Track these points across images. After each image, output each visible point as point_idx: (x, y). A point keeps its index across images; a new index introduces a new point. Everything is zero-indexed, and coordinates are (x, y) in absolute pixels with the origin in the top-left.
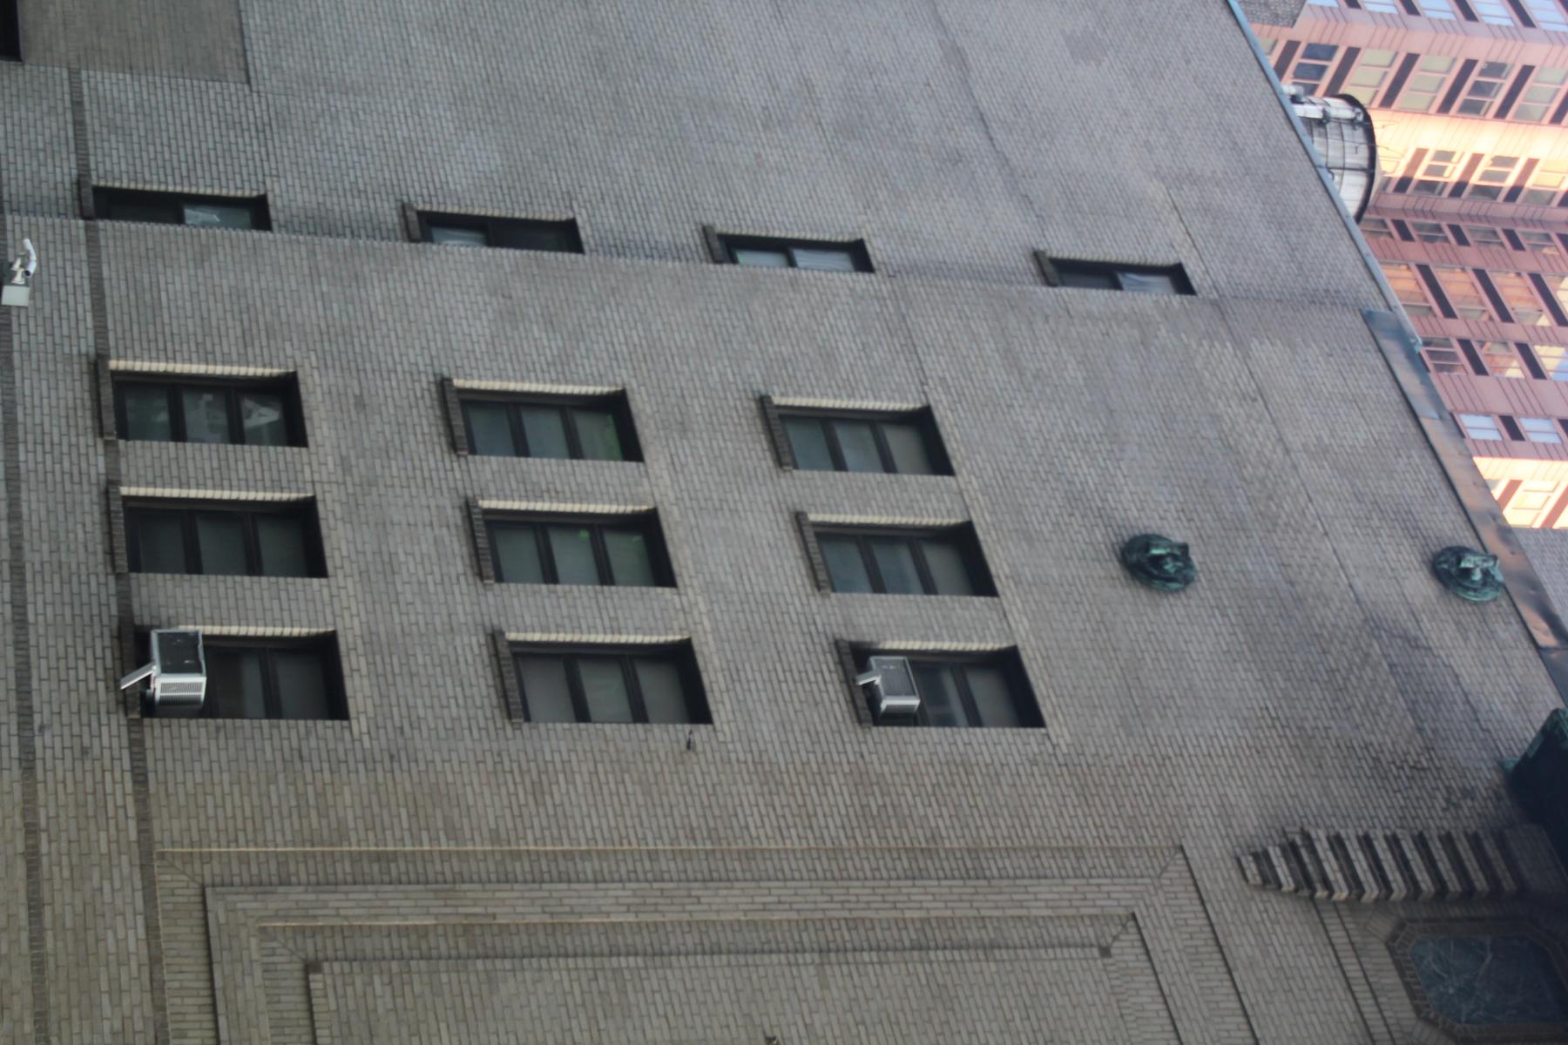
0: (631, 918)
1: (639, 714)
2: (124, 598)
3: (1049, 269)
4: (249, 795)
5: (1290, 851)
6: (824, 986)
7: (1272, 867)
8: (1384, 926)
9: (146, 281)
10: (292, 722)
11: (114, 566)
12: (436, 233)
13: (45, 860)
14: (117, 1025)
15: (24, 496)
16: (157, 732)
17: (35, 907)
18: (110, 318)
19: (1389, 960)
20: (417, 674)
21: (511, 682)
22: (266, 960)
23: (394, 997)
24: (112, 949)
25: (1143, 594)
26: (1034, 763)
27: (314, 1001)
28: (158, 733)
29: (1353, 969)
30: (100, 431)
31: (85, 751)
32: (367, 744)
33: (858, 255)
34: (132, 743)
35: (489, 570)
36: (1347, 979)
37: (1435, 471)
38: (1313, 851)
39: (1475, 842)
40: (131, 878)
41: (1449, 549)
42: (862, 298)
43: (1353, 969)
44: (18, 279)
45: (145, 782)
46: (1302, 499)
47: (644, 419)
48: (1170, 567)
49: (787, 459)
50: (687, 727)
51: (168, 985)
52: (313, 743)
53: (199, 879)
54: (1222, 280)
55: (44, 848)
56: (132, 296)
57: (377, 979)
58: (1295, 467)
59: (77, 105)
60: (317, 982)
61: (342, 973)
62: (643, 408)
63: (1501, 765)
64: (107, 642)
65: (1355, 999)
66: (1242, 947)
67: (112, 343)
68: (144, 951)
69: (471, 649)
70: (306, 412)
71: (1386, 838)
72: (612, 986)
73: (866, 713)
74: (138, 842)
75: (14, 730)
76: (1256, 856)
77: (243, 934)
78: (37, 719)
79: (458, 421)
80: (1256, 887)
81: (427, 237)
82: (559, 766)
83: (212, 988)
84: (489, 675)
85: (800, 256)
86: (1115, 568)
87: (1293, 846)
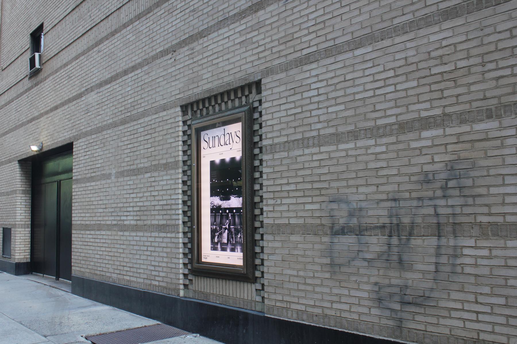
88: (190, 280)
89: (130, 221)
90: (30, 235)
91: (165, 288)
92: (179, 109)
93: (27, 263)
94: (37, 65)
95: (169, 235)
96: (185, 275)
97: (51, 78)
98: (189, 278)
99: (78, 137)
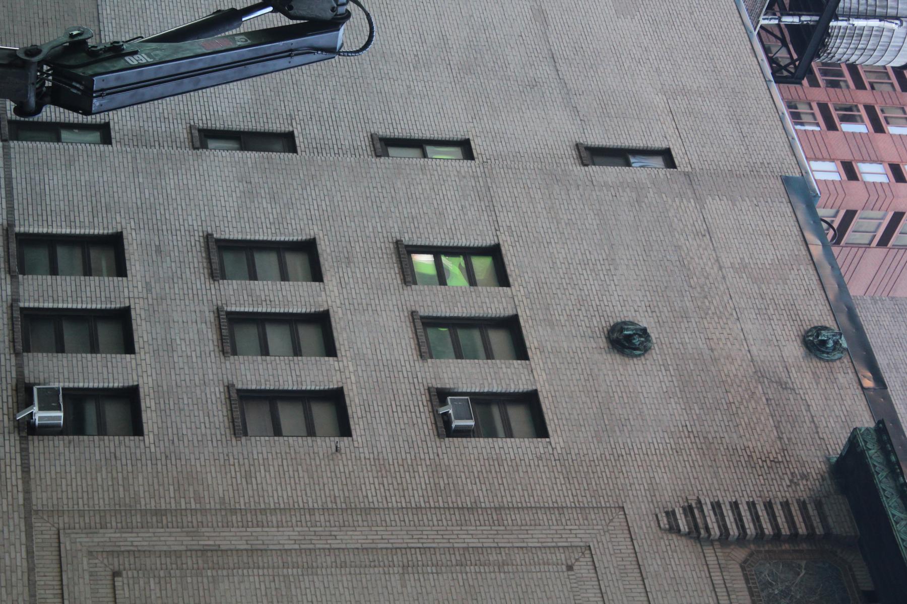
0: (297, 547)
1: (311, 432)
2: (20, 367)
3: (584, 154)
4: (86, 479)
5: (689, 510)
6: (404, 586)
7: (676, 520)
8: (740, 554)
9: (37, 178)
10: (111, 437)
11: (14, 350)
12: (212, 144)
16: (36, 444)
18: (16, 201)
19: (741, 574)
20: (184, 410)
21: (237, 414)
22: (91, 570)
23: (161, 590)
24: (8, 563)
25: (618, 358)
26: (540, 459)
27: (117, 592)
28: (37, 445)
29: (717, 579)
30: (9, 271)
32: (153, 450)
34: (22, 450)
35: (228, 348)
36: (713, 584)
37: (815, 278)
38: (702, 511)
39: (803, 505)
40: (19, 525)
41: (815, 328)
42: (464, 177)
43: (717, 579)
45: (29, 472)
47: (325, 256)
48: (637, 341)
49: (409, 279)
50: (337, 439)
51: (38, 583)
53: (56, 525)
54: (695, 158)
56: (29, 188)
57: (152, 580)
58: (724, 278)
60: (118, 584)
61: (133, 577)
64: (10, 393)
65: (717, 596)
66: (652, 565)
67: (17, 218)
68: (25, 564)
69: (215, 395)
70: (127, 256)
71: (748, 503)
72: (283, 584)
74: (24, 505)
76: (667, 513)
77: (80, 555)
79: (215, 259)
80: (665, 530)
81: (204, 146)
82: (261, 462)
83: (62, 585)
84: (225, 410)
85: (429, 149)
86: (603, 343)
87: (690, 507)
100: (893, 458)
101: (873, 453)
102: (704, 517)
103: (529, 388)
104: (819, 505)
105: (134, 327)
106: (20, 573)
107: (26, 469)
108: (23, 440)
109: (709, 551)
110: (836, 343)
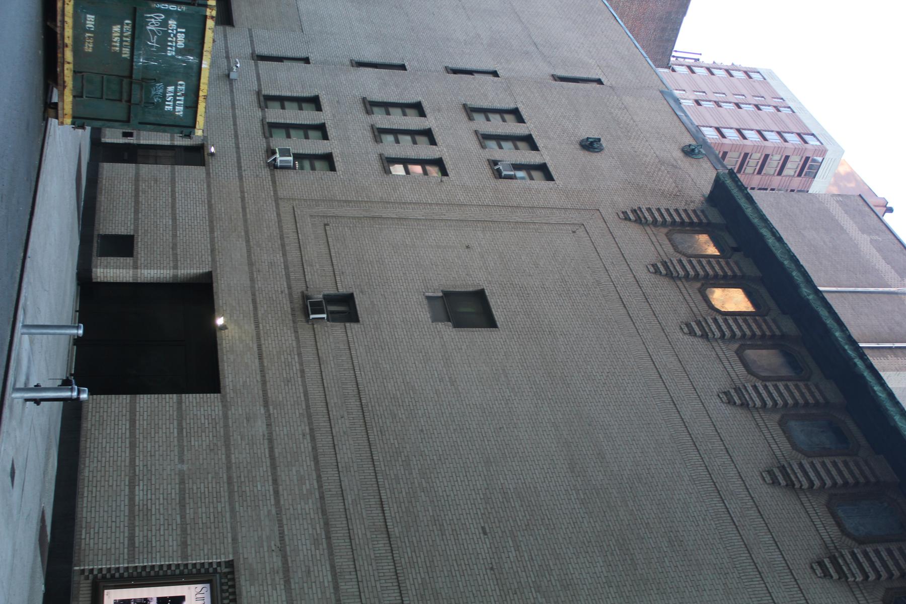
13: (246, 199)
14: (269, 234)
15: (238, 120)
17: (244, 208)
25: (587, 153)
26: (551, 189)
28: (278, 173)
31: (257, 176)
32: (342, 177)
33: (495, 74)
38: (641, 211)
44: (235, 70)
46: (639, 133)
52: (325, 176)
54: (614, 83)
55: (246, 195)
57: (346, 228)
59: (251, 36)
60: (327, 228)
62: (425, 105)
63: (703, 196)
68: (276, 218)
73: (498, 176)
75: (236, 170)
76: (623, 212)
78: (243, 169)
83: (297, 228)
86: (578, 146)
88: (88, 576)
89: (139, 495)
90: (124, 281)
91: (80, 549)
92: (231, 558)
93: (91, 278)
94: (312, 316)
95: (126, 550)
96: (92, 571)
97: (294, 344)
98: (90, 575)
99: (224, 401)
100: (740, 183)
101: (728, 182)
102: (643, 213)
103: (542, 162)
104: (703, 211)
105: (328, 130)
106: (273, 223)
107: (274, 182)
108: (271, 170)
109: (647, 228)
110: (700, 151)
